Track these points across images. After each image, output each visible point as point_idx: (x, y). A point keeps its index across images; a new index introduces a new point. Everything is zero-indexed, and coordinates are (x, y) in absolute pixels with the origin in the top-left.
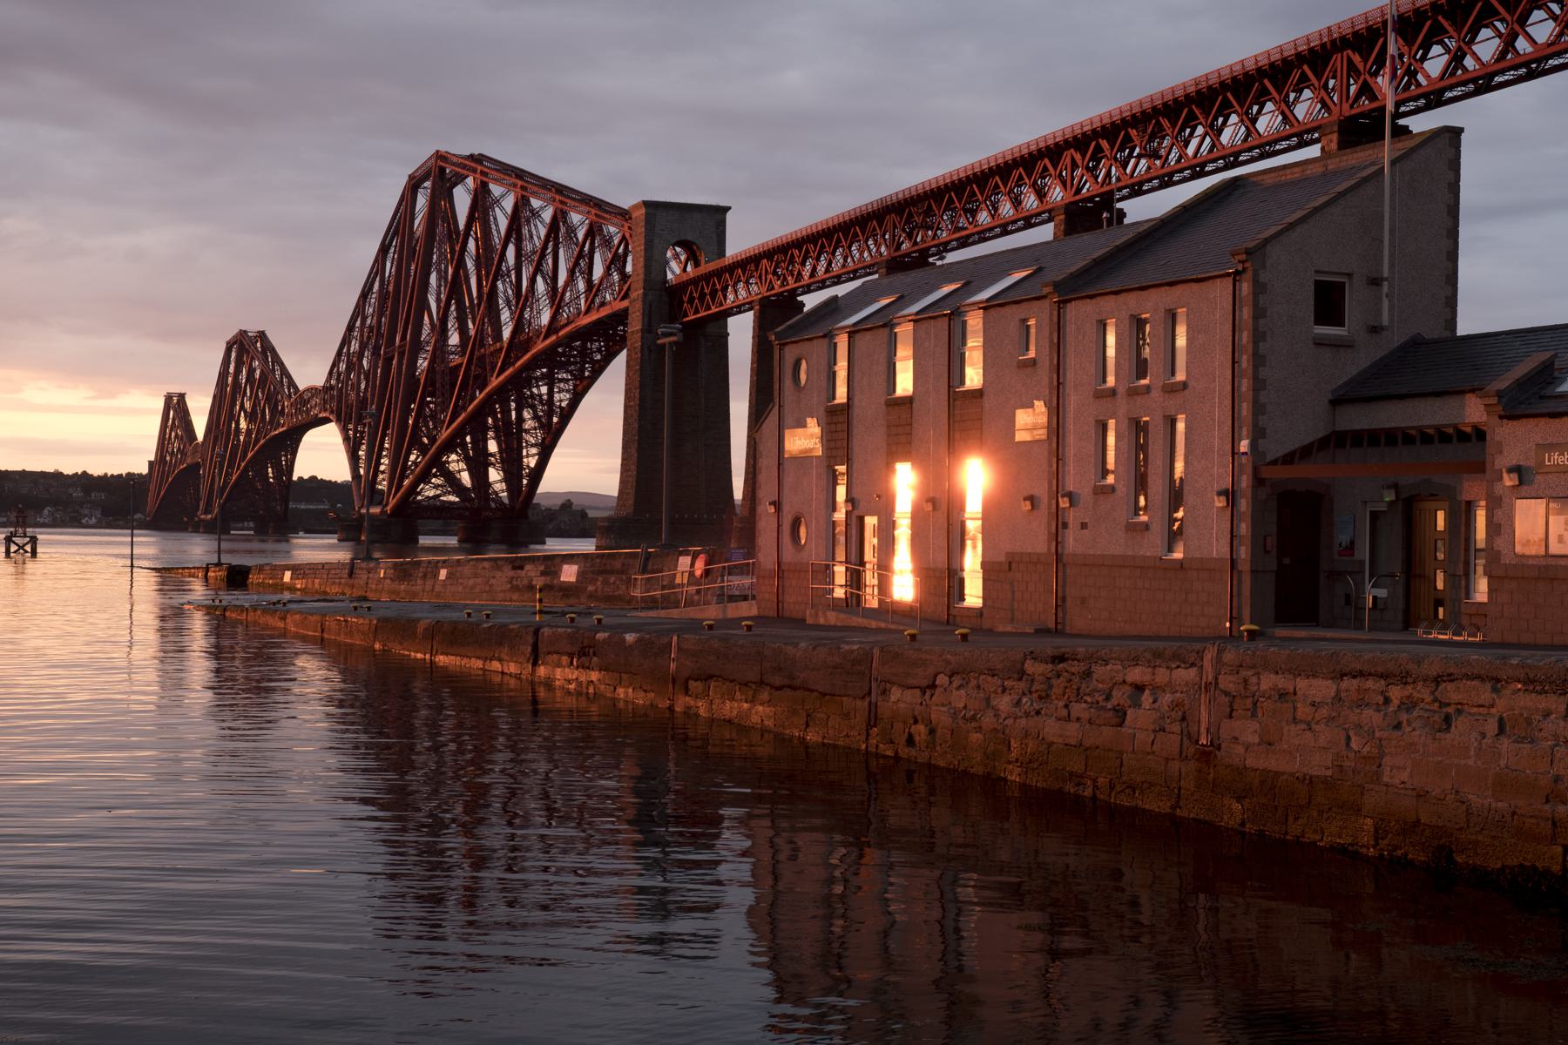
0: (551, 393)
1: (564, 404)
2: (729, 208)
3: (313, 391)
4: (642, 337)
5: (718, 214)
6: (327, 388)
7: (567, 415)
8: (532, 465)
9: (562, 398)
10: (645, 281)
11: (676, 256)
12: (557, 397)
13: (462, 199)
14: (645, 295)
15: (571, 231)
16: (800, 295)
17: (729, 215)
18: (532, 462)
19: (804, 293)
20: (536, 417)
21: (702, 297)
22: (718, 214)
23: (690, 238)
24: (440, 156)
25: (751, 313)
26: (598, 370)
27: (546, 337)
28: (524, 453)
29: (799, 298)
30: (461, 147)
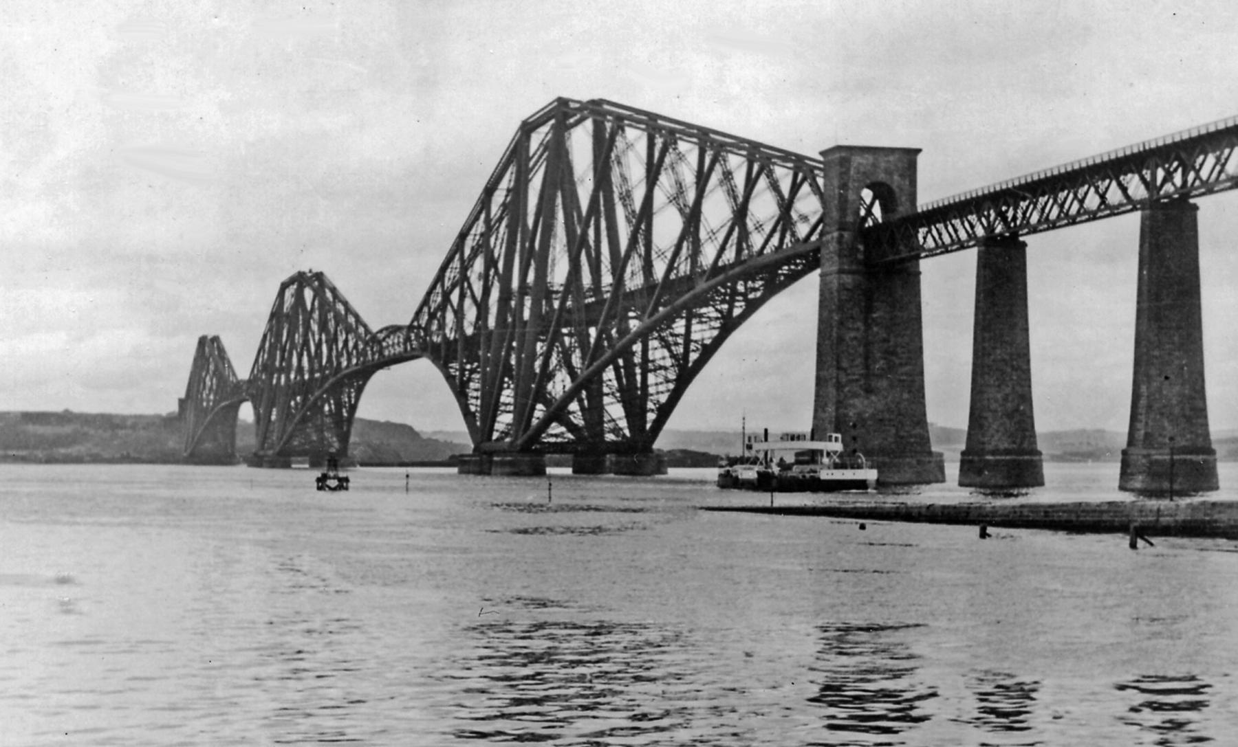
1: (708, 342)
2: (918, 151)
3: (393, 330)
5: (911, 155)
6: (410, 328)
7: (708, 351)
9: (703, 333)
12: (694, 336)
13: (581, 142)
15: (728, 175)
16: (1022, 235)
17: (921, 159)
18: (663, 398)
22: (911, 155)
23: (882, 177)
24: (562, 102)
27: (707, 280)
28: (651, 390)
30: (581, 93)
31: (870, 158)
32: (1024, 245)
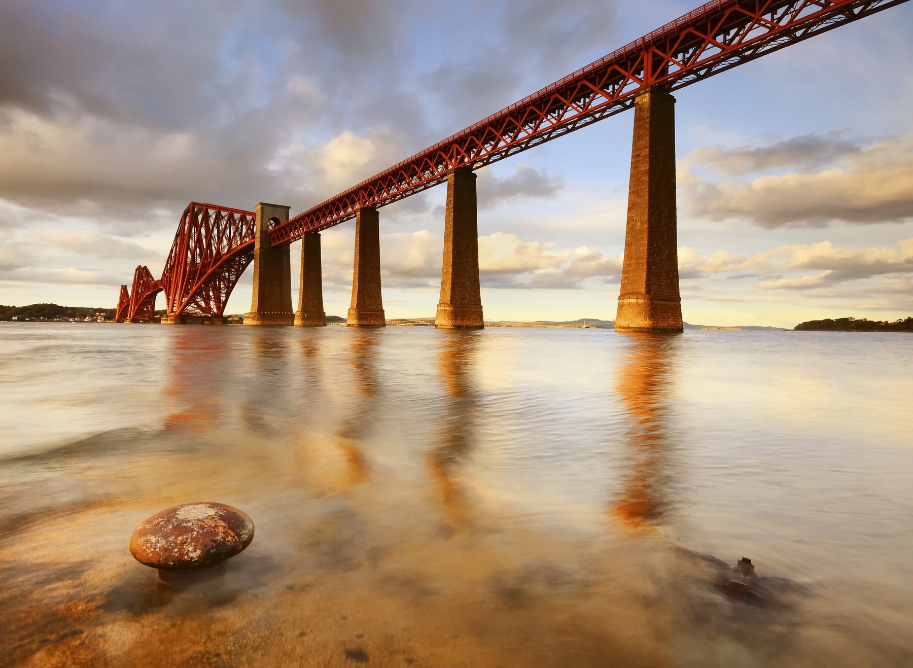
0: (229, 276)
2: (290, 207)
4: (260, 250)
5: (287, 208)
7: (234, 283)
8: (223, 300)
9: (233, 278)
10: (261, 231)
11: (271, 225)
14: (261, 236)
18: (223, 299)
19: (320, 231)
20: (225, 285)
21: (282, 235)
22: (287, 208)
23: (277, 216)
25: (301, 240)
26: (245, 266)
29: (319, 233)
31: (270, 208)
32: (320, 235)
